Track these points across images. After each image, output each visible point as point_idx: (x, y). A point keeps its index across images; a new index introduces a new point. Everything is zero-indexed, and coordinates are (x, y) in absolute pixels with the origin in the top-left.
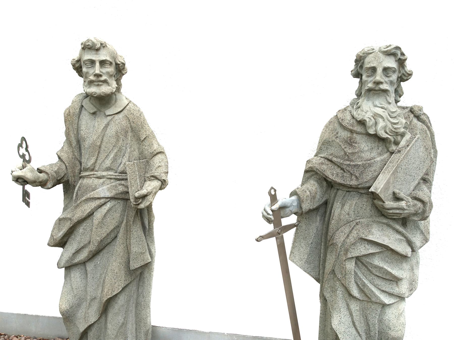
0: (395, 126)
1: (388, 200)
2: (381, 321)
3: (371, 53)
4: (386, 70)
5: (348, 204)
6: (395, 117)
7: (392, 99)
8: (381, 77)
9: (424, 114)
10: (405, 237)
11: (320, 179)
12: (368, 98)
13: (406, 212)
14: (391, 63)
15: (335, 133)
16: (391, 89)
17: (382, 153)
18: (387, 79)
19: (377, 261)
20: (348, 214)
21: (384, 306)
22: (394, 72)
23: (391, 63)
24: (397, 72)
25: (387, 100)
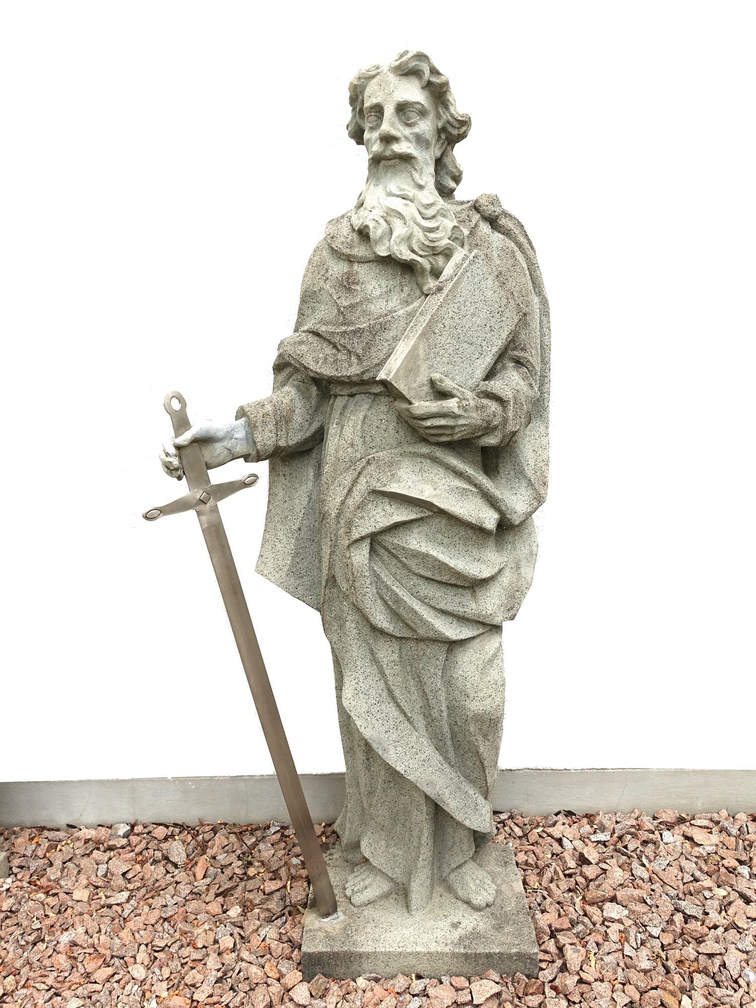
1: (421, 398)
2: (449, 683)
4: (402, 108)
5: (351, 423)
6: (434, 217)
7: (427, 177)
8: (392, 125)
9: (506, 214)
10: (475, 485)
11: (303, 382)
12: (378, 179)
13: (461, 422)
14: (412, 92)
15: (323, 272)
16: (425, 158)
17: (410, 300)
18: (407, 131)
19: (416, 541)
20: (352, 445)
21: (453, 645)
22: (423, 113)
23: (412, 92)
24: (432, 115)
25: (413, 180)
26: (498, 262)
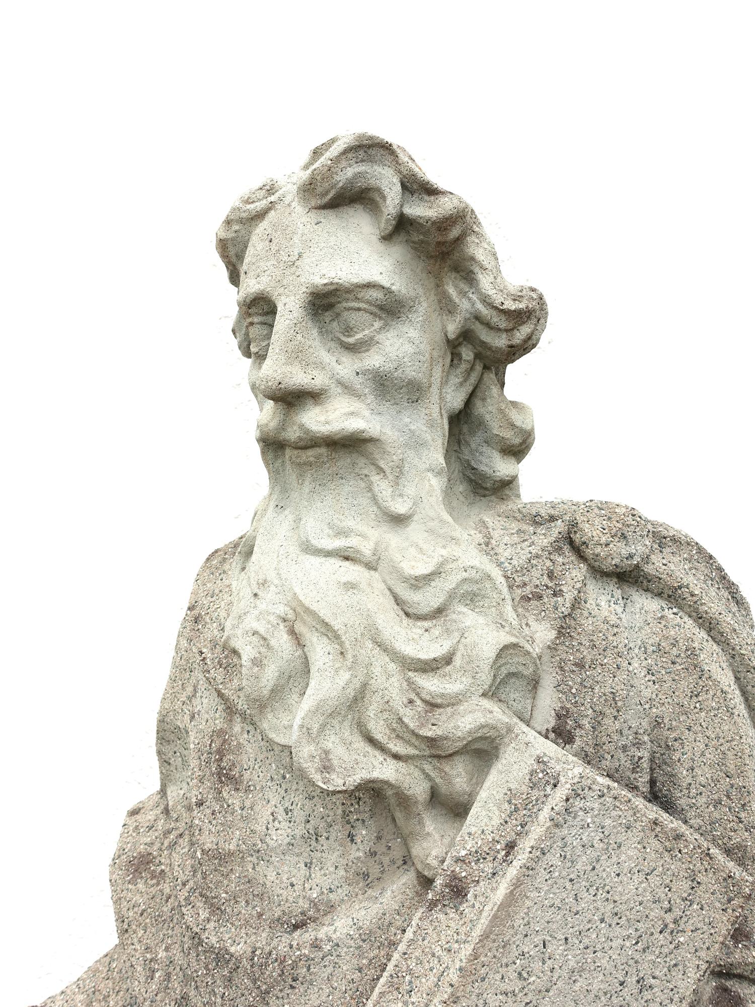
0: (431, 684)
4: (324, 303)
6: (439, 612)
14: (356, 254)
17: (375, 871)
18: (346, 367)
22: (391, 309)
23: (356, 254)
24: (424, 307)
25: (374, 499)
26: (647, 693)
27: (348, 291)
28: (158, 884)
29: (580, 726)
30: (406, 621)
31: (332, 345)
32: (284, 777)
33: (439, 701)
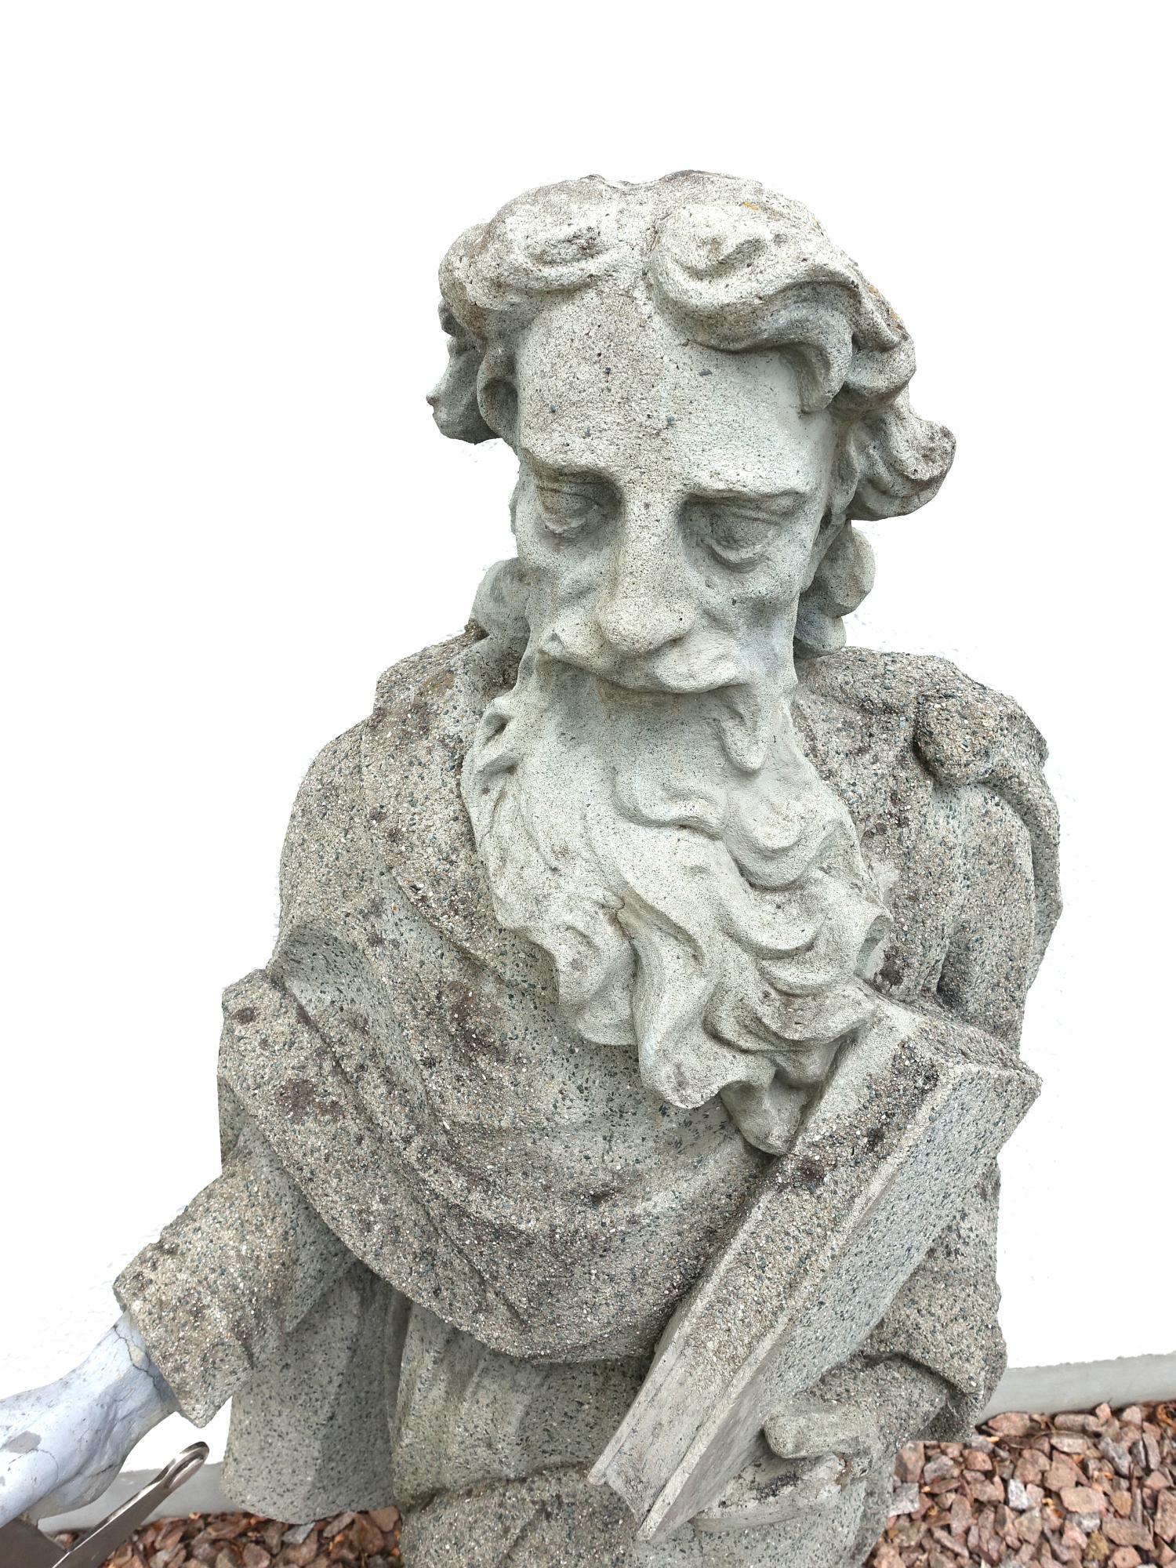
3: (568, 292)
4: (713, 519)
15: (362, 902)
25: (724, 750)
27: (750, 500)
28: (335, 1120)
29: (908, 966)
30: (753, 894)
31: (698, 553)
32: (572, 1051)
33: (798, 992)
